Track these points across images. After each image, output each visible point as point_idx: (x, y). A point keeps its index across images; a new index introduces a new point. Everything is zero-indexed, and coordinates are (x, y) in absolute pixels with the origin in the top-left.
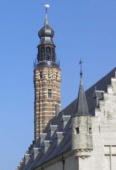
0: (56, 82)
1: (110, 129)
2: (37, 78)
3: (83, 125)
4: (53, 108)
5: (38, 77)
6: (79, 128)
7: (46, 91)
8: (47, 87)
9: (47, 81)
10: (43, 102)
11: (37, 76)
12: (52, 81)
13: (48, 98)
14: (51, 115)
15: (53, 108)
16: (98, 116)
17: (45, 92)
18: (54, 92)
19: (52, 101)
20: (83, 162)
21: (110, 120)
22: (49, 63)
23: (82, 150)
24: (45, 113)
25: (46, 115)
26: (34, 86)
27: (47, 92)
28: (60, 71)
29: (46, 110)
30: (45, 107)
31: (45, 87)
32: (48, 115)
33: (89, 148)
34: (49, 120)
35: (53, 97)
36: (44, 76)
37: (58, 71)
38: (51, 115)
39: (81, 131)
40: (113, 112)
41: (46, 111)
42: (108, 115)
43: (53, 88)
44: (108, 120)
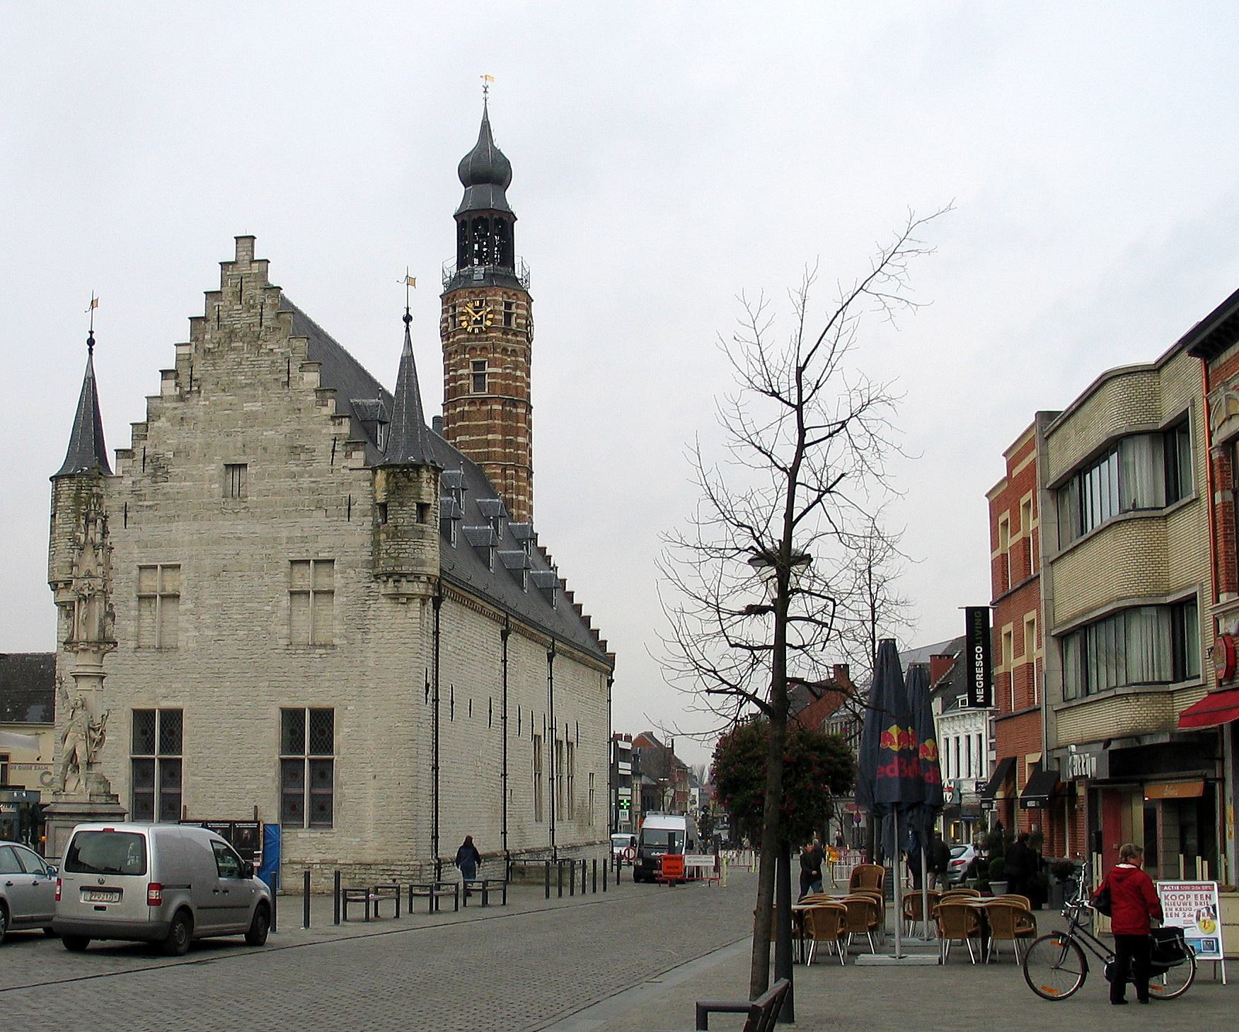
1: (160, 514)
3: (64, 508)
16: (123, 472)
21: (160, 484)
37: (514, 295)
40: (172, 456)
42: (154, 469)
44: (156, 482)
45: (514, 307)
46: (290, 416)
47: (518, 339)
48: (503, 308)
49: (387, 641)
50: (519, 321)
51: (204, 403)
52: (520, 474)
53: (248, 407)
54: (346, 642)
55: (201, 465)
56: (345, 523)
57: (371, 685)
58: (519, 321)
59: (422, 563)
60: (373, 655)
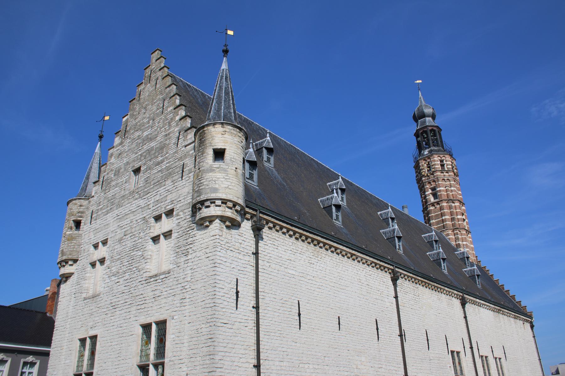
7: (428, 191)
8: (427, 186)
13: (432, 200)
14: (440, 225)
16: (95, 194)
17: (427, 193)
18: (438, 189)
29: (431, 219)
32: (437, 226)
33: (64, 258)
38: (440, 225)
40: (113, 176)
45: (444, 161)
46: (162, 130)
47: (449, 174)
48: (439, 163)
49: (198, 259)
50: (448, 167)
51: (129, 141)
52: (462, 232)
53: (145, 134)
54: (175, 266)
55: (123, 176)
57: (188, 297)
58: (448, 167)
59: (215, 190)
60: (190, 272)
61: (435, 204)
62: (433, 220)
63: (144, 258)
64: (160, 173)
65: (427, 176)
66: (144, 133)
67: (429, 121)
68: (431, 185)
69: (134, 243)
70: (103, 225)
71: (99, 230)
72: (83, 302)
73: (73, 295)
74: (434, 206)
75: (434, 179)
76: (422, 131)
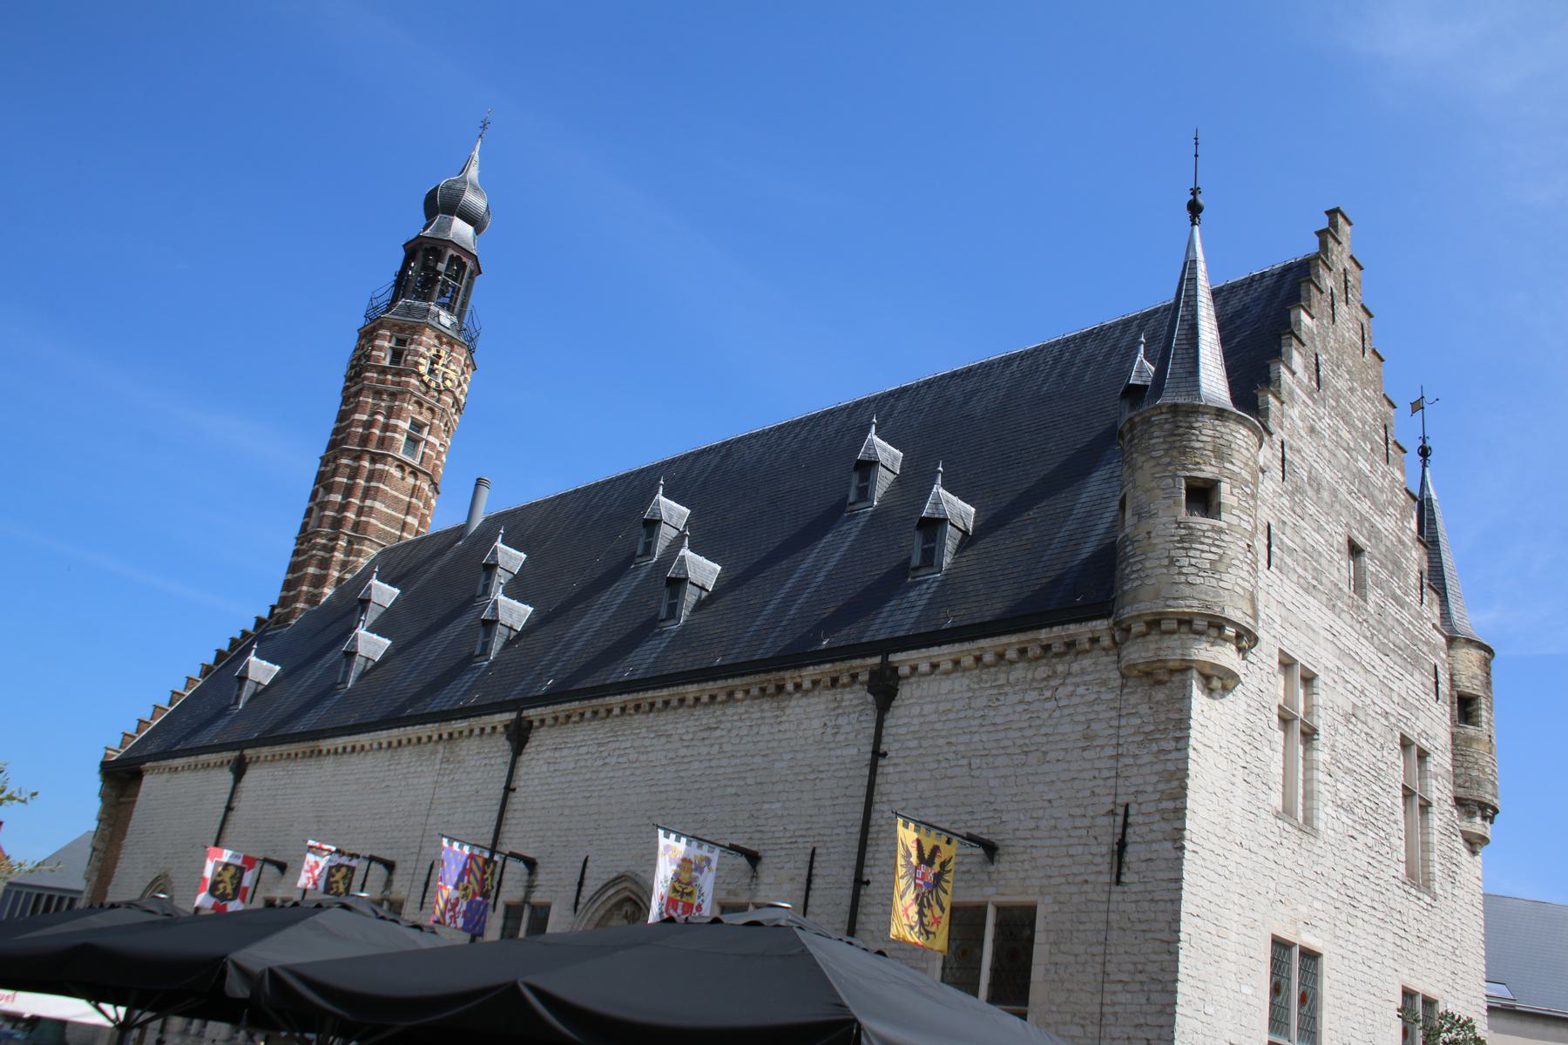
0: (450, 401)
2: (378, 359)
4: (410, 503)
5: (383, 355)
6: (1222, 484)
7: (406, 421)
8: (410, 408)
9: (417, 383)
10: (373, 461)
11: (381, 349)
12: (440, 392)
14: (393, 531)
15: (410, 503)
18: (431, 439)
19: (415, 473)
20: (1207, 714)
22: (446, 319)
23: (1230, 631)
24: (371, 508)
25: (373, 521)
26: (346, 389)
27: (405, 425)
28: (470, 370)
29: (379, 498)
30: (381, 486)
31: (406, 405)
32: (382, 526)
34: (381, 549)
35: (422, 458)
36: (416, 358)
39: (1233, 507)
40: (1306, 479)
41: (378, 505)
43: (435, 421)
56: (1434, 704)
61: (408, 470)
62: (383, 503)
63: (1395, 822)
64: (1400, 629)
65: (427, 386)
66: (1360, 458)
67: (461, 230)
68: (421, 413)
69: (1374, 760)
70: (1302, 617)
71: (1293, 619)
72: (1272, 819)
73: (1242, 770)
74: (403, 470)
75: (434, 405)
76: (455, 254)
